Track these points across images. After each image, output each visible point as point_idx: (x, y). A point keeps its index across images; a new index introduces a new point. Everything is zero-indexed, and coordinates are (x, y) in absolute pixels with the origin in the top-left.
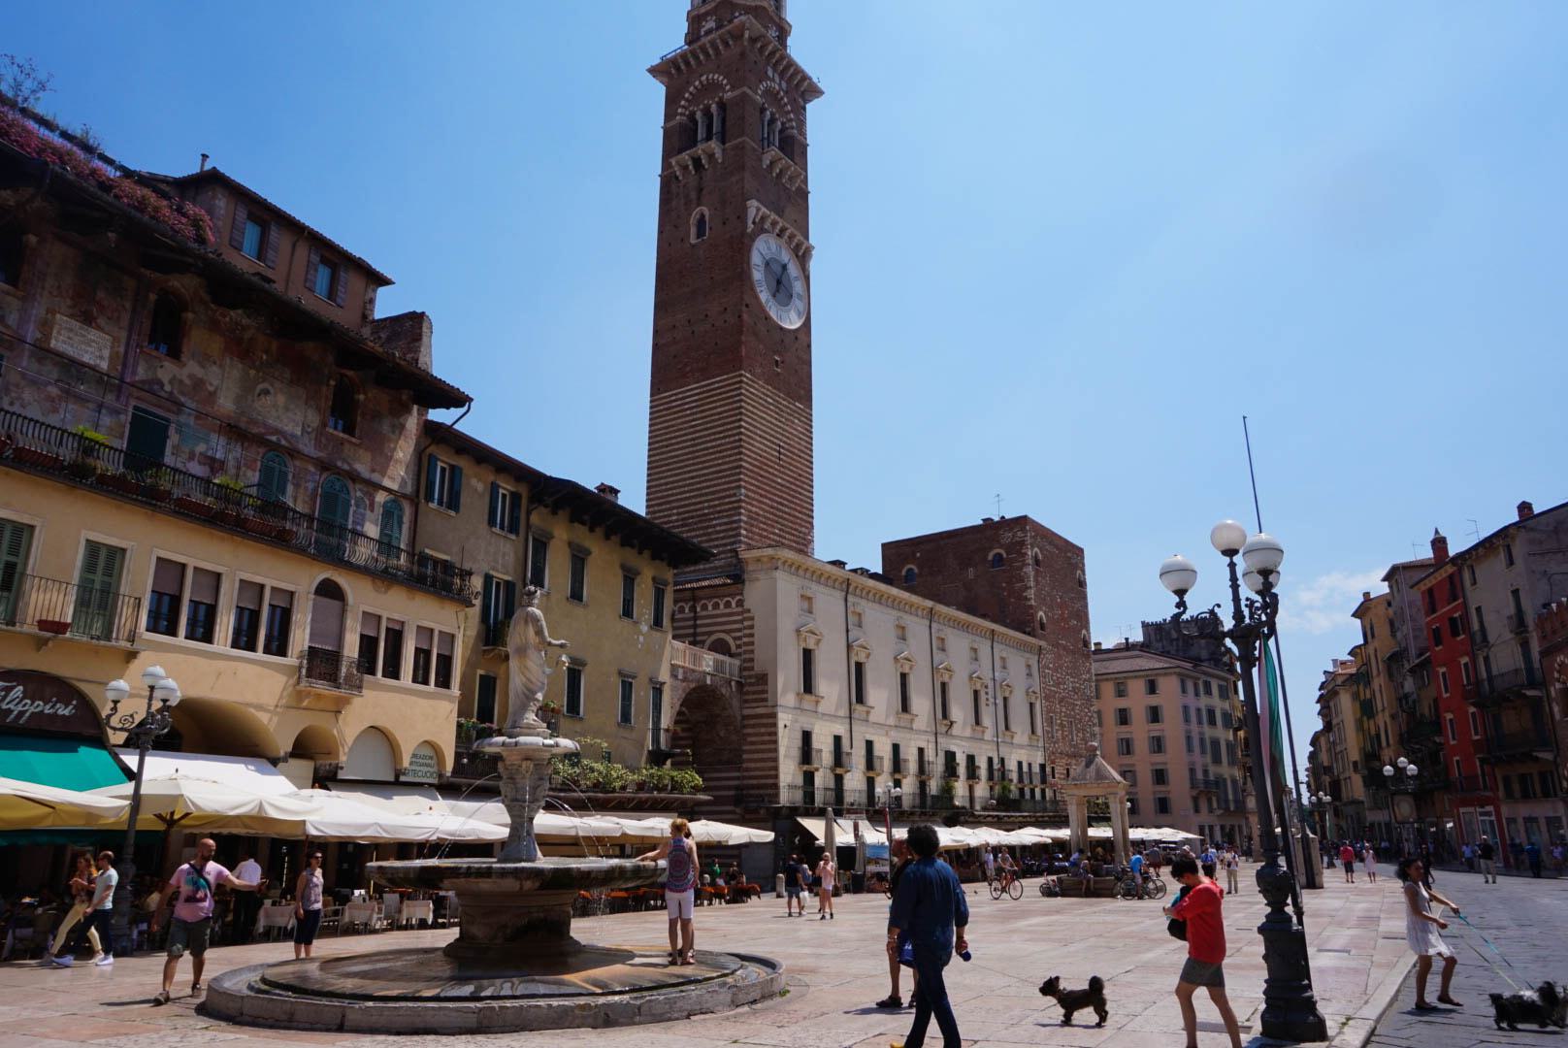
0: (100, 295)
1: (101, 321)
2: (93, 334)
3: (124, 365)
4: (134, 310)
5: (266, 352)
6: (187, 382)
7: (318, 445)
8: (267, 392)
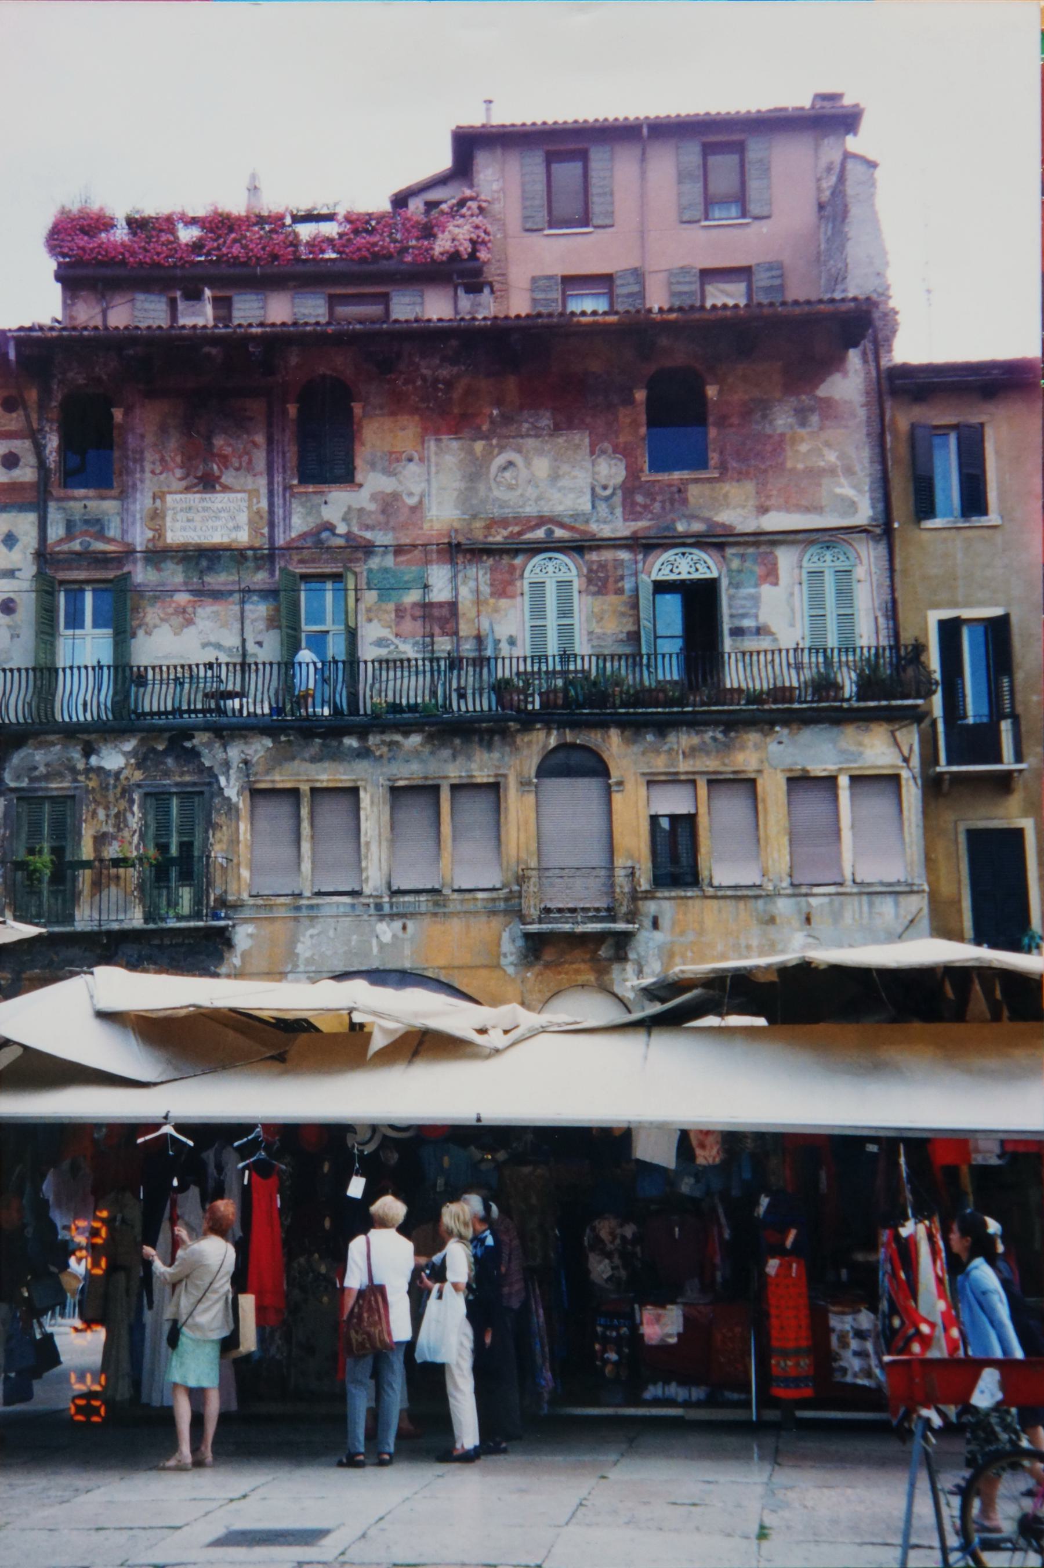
0: (219, 442)
2: (219, 500)
3: (272, 525)
4: (270, 441)
5: (499, 403)
6: (372, 507)
7: (631, 511)
8: (511, 464)
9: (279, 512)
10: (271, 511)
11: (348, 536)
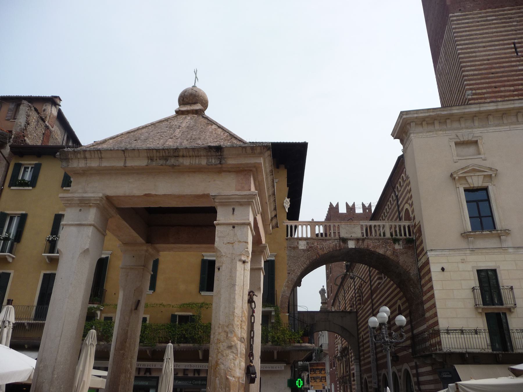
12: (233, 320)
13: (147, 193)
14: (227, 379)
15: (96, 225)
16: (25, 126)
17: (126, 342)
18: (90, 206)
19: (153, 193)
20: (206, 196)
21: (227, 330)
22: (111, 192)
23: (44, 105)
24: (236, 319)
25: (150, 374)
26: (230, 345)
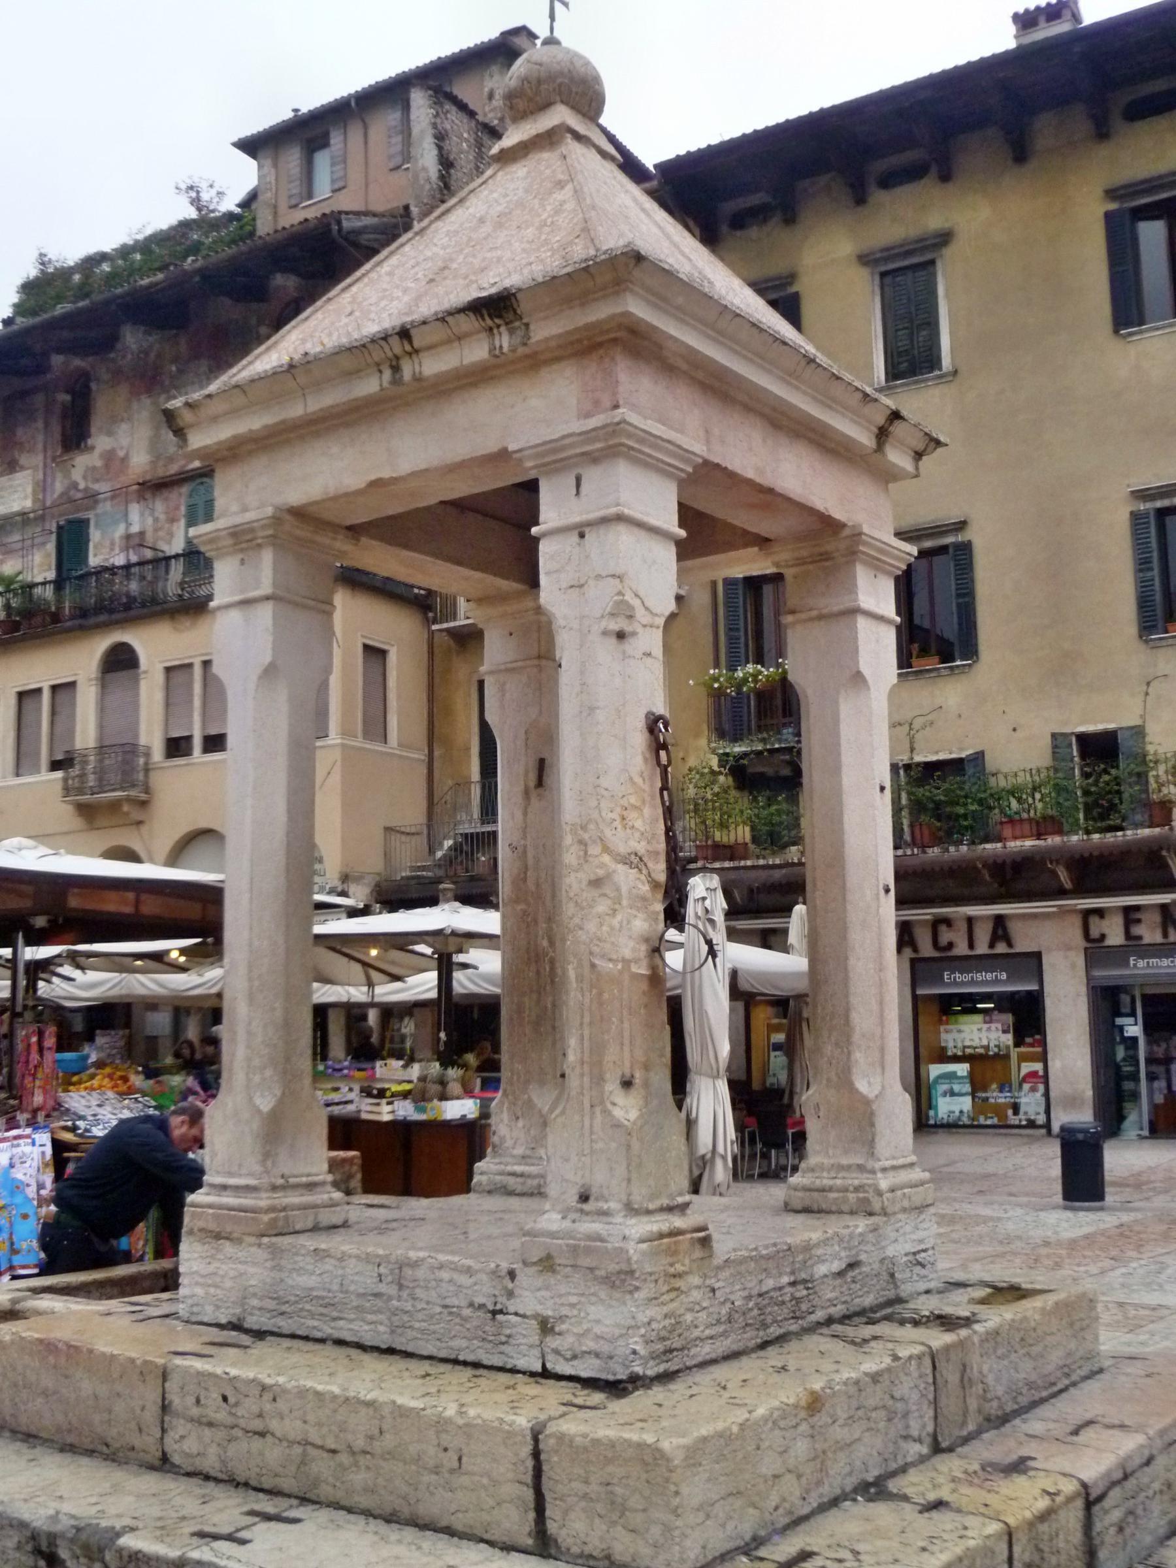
0: (20, 432)
1: (24, 460)
5: (175, 360)
9: (49, 480)
10: (45, 481)
11: (86, 489)
12: (598, 807)
13: (373, 477)
14: (593, 966)
15: (280, 593)
16: (442, 177)
17: (525, 880)
18: (259, 546)
19: (386, 474)
20: (503, 455)
21: (586, 836)
22: (295, 496)
23: (487, 77)
24: (604, 805)
25: (1010, 945)
26: (593, 877)
